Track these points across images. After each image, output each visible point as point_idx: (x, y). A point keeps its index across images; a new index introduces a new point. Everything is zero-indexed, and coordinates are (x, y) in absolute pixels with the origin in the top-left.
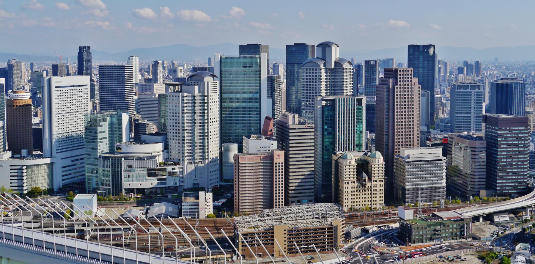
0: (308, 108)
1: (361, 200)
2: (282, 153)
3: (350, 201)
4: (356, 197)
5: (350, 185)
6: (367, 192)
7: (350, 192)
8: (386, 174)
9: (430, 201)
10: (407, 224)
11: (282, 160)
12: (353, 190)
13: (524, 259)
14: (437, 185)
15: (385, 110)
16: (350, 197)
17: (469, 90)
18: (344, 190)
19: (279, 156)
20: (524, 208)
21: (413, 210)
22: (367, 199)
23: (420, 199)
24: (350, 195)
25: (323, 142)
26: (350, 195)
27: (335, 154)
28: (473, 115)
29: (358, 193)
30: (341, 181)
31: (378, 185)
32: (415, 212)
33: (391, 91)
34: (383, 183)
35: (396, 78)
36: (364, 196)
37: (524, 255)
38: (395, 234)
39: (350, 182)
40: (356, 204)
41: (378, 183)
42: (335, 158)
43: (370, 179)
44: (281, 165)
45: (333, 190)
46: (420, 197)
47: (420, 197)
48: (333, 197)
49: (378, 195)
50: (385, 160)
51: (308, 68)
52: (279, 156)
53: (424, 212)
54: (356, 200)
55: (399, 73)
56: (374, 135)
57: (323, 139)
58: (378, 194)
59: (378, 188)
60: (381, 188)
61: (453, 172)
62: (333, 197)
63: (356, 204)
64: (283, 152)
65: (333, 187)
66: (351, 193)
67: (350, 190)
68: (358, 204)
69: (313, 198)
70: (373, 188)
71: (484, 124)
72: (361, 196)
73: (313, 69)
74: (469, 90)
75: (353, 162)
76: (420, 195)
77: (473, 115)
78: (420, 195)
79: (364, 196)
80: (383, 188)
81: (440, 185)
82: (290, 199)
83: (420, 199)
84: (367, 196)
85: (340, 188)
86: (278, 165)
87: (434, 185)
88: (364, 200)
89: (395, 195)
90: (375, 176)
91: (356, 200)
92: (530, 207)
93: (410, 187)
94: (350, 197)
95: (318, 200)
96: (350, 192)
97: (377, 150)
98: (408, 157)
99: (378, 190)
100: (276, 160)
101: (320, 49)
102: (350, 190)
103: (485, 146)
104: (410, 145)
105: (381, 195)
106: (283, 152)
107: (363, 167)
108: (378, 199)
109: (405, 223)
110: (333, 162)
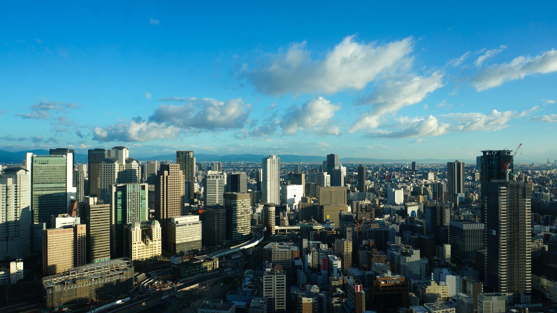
5: (137, 245)
6: (149, 249)
13: (249, 279)
17: (215, 179)
19: (82, 228)
35: (168, 170)
37: (249, 277)
43: (151, 239)
50: (161, 226)
52: (82, 228)
59: (157, 245)
67: (137, 249)
72: (145, 252)
74: (215, 179)
84: (149, 251)
96: (137, 250)
98: (177, 222)
102: (137, 249)
103: (225, 212)
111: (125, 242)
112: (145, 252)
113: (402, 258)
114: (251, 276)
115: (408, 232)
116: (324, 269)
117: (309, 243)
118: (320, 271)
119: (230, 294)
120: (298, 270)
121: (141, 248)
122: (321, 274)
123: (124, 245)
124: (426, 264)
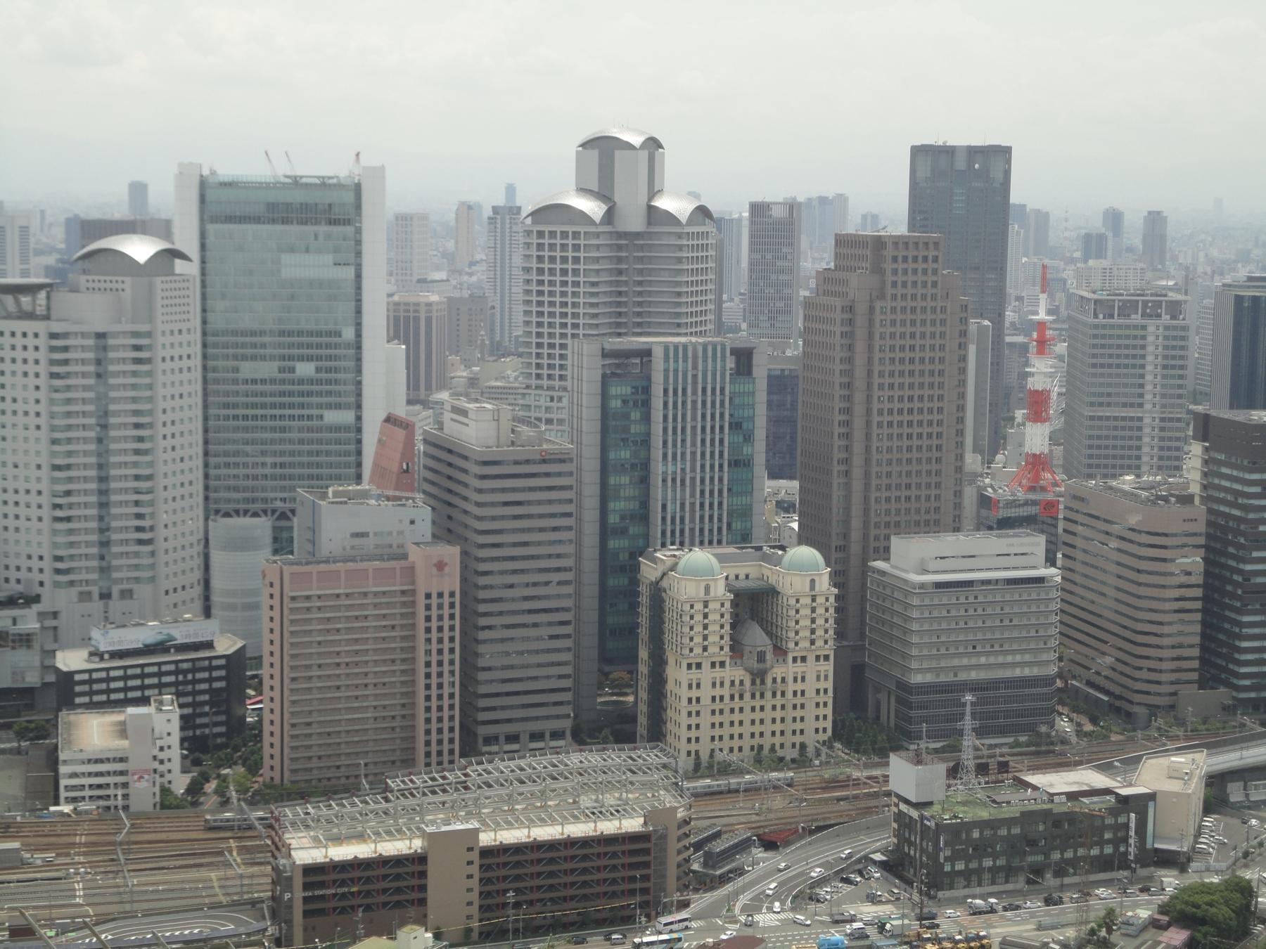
0: (545, 383)
1: (747, 729)
2: (451, 553)
3: (705, 733)
4: (726, 718)
5: (706, 675)
6: (768, 702)
7: (706, 700)
8: (840, 635)
9: (1002, 731)
10: (922, 817)
11: (452, 581)
12: (718, 692)
14: (1027, 672)
15: (838, 392)
16: (705, 720)
17: (1136, 319)
18: (685, 693)
19: (440, 566)
21: (942, 768)
22: (768, 728)
23: (968, 723)
24: (706, 714)
26: (706, 714)
27: (655, 560)
28: (1150, 414)
29: (737, 704)
30: (671, 661)
31: (810, 677)
32: (953, 772)
33: (861, 321)
34: (829, 667)
35: (878, 270)
36: (757, 716)
38: (878, 857)
39: (706, 665)
40: (727, 743)
41: (811, 668)
42: (649, 572)
43: (780, 651)
44: (446, 600)
45: (643, 695)
46: (968, 717)
47: (968, 717)
48: (642, 720)
49: (810, 712)
50: (839, 578)
51: (546, 228)
52: (440, 566)
53: (982, 769)
54: (726, 731)
55: (889, 252)
56: (789, 487)
58: (810, 706)
59: (810, 686)
60: (822, 685)
61: (1080, 624)
62: (642, 720)
63: (727, 743)
64: (456, 550)
65: (643, 683)
67: (706, 693)
68: (736, 743)
69: (567, 724)
70: (791, 687)
71: (1196, 449)
72: (747, 716)
73: (564, 235)
74: (1136, 319)
75: (719, 590)
76: (968, 709)
77: (1150, 414)
78: (968, 709)
79: (757, 716)
80: (830, 685)
81: (1035, 671)
82: (483, 731)
83: (968, 723)
84: (768, 715)
85: (670, 686)
86: (434, 601)
87: (1018, 672)
88: (757, 729)
89: (872, 709)
90: (798, 642)
91: (726, 731)
93: (929, 678)
94: (705, 720)
95: (583, 736)
96: (706, 700)
97: (805, 538)
99: (810, 693)
101: (594, 154)
102: (706, 693)
103: (1201, 527)
104: (930, 524)
105: (821, 711)
106: (456, 550)
108: (810, 725)
109: (915, 814)
110: (644, 589)
111: (643, 654)
112: (747, 716)
121: (726, 692)
123: (643, 669)
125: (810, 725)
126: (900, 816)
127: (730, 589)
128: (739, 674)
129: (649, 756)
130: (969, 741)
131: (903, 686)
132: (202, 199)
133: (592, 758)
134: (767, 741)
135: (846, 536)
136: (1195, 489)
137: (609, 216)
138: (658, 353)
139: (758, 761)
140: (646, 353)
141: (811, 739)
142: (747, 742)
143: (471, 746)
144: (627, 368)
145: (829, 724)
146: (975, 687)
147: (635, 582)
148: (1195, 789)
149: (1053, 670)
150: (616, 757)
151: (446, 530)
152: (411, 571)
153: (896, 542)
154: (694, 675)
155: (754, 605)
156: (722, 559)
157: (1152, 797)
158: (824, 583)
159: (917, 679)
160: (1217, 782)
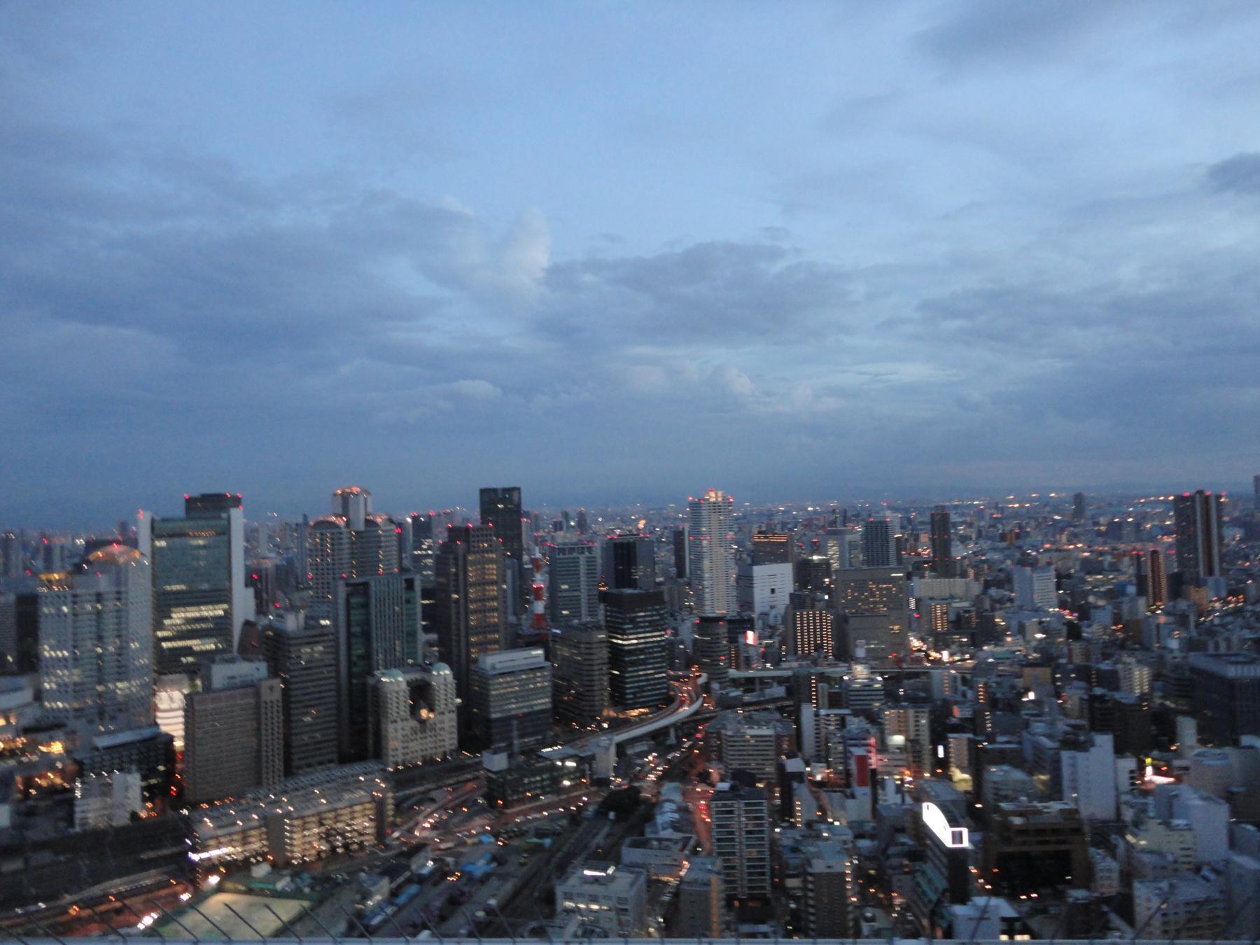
3: (399, 753)
5: (400, 725)
11: (277, 695)
13: (674, 807)
17: (575, 555)
20: (666, 728)
23: (515, 733)
25: (349, 655)
32: (510, 756)
33: (460, 563)
34: (454, 716)
35: (467, 541)
42: (371, 681)
50: (457, 676)
52: (271, 688)
53: (523, 753)
56: (433, 637)
57: (349, 648)
59: (446, 726)
66: (401, 740)
69: (335, 756)
70: (439, 726)
71: (602, 606)
74: (575, 555)
75: (404, 686)
82: (295, 763)
83: (515, 733)
87: (536, 708)
90: (440, 705)
92: (674, 725)
95: (344, 760)
98: (493, 668)
100: (267, 696)
107: (421, 693)
108: (447, 743)
113: (1066, 755)
114: (678, 798)
115: (1076, 683)
116: (862, 783)
117: (817, 715)
118: (848, 785)
119: (635, 845)
120: (795, 785)
122: (853, 796)
124: (1132, 772)
125: (447, 743)
126: (489, 780)
127: (409, 684)
128: (414, 723)
129: (372, 765)
130: (516, 742)
131: (489, 721)
132: (153, 529)
133: (347, 770)
134: (430, 751)
135: (459, 656)
136: (603, 623)
137: (348, 524)
138: (373, 584)
139: (424, 762)
140: (366, 585)
141: (448, 748)
142: (421, 753)
143: (289, 771)
144: (360, 590)
145: (455, 742)
146: (516, 717)
147: (364, 685)
148: (613, 750)
149: (549, 706)
150: (357, 767)
151: (274, 672)
152: (257, 694)
153: (481, 658)
154: (394, 725)
155: (421, 693)
156: (404, 672)
157: (593, 757)
158: (450, 679)
159: (494, 716)
160: (621, 747)
